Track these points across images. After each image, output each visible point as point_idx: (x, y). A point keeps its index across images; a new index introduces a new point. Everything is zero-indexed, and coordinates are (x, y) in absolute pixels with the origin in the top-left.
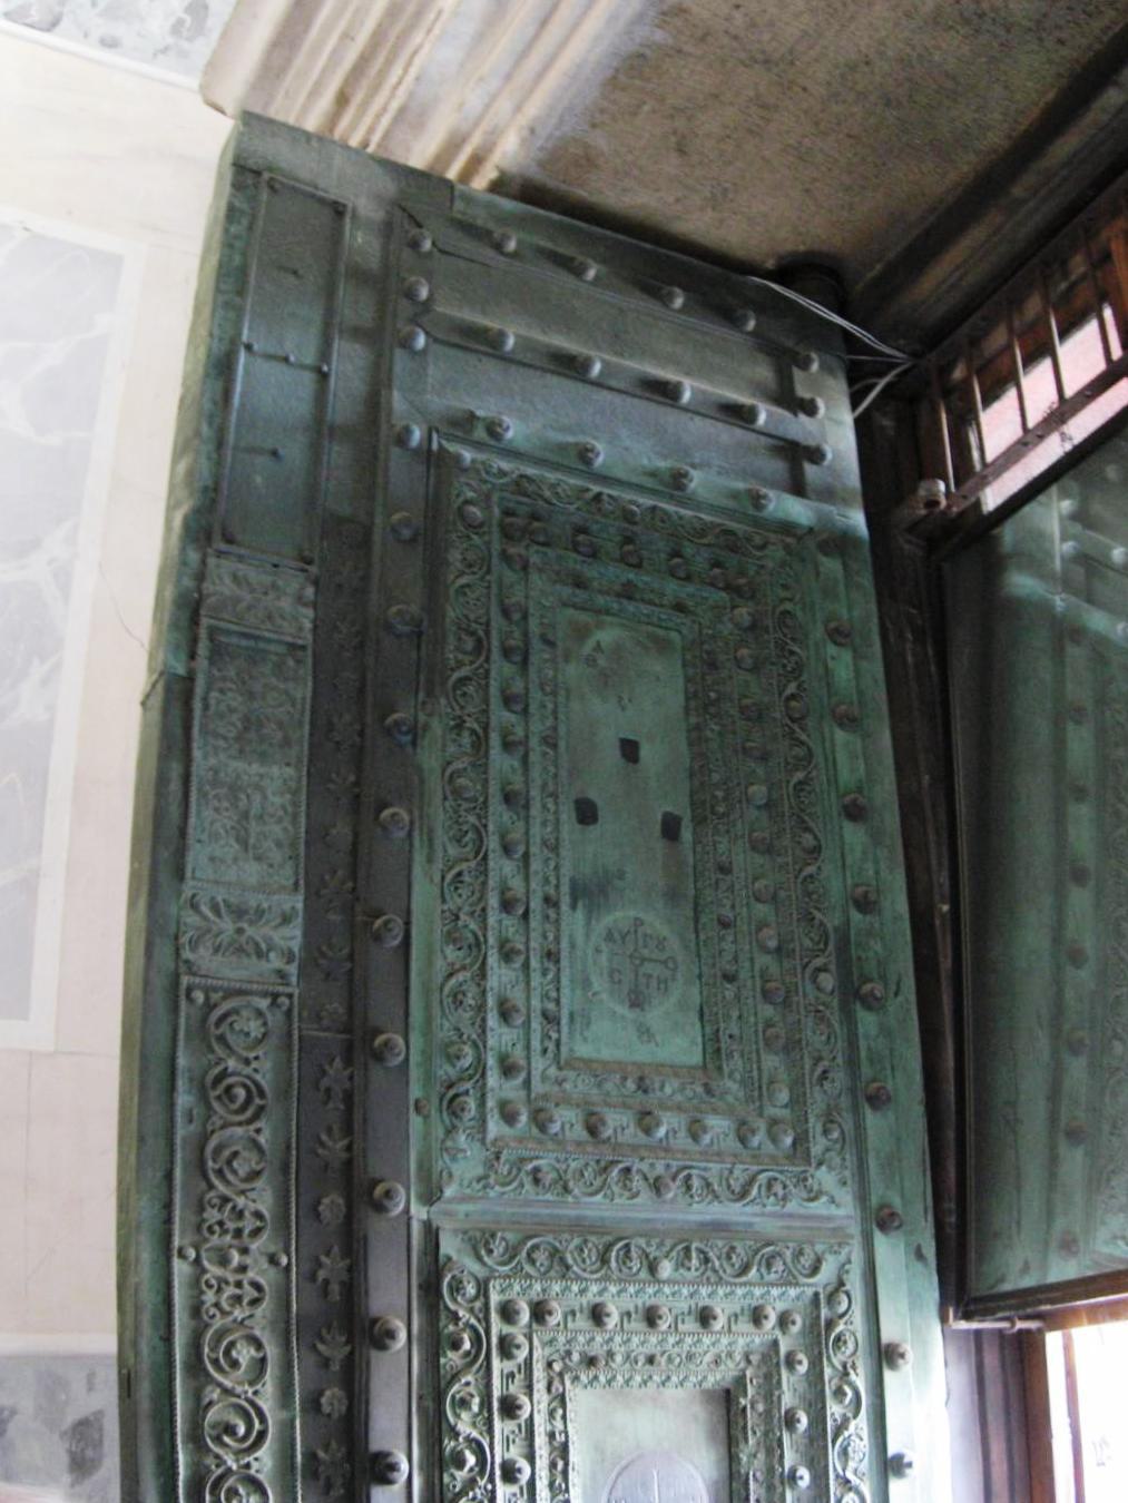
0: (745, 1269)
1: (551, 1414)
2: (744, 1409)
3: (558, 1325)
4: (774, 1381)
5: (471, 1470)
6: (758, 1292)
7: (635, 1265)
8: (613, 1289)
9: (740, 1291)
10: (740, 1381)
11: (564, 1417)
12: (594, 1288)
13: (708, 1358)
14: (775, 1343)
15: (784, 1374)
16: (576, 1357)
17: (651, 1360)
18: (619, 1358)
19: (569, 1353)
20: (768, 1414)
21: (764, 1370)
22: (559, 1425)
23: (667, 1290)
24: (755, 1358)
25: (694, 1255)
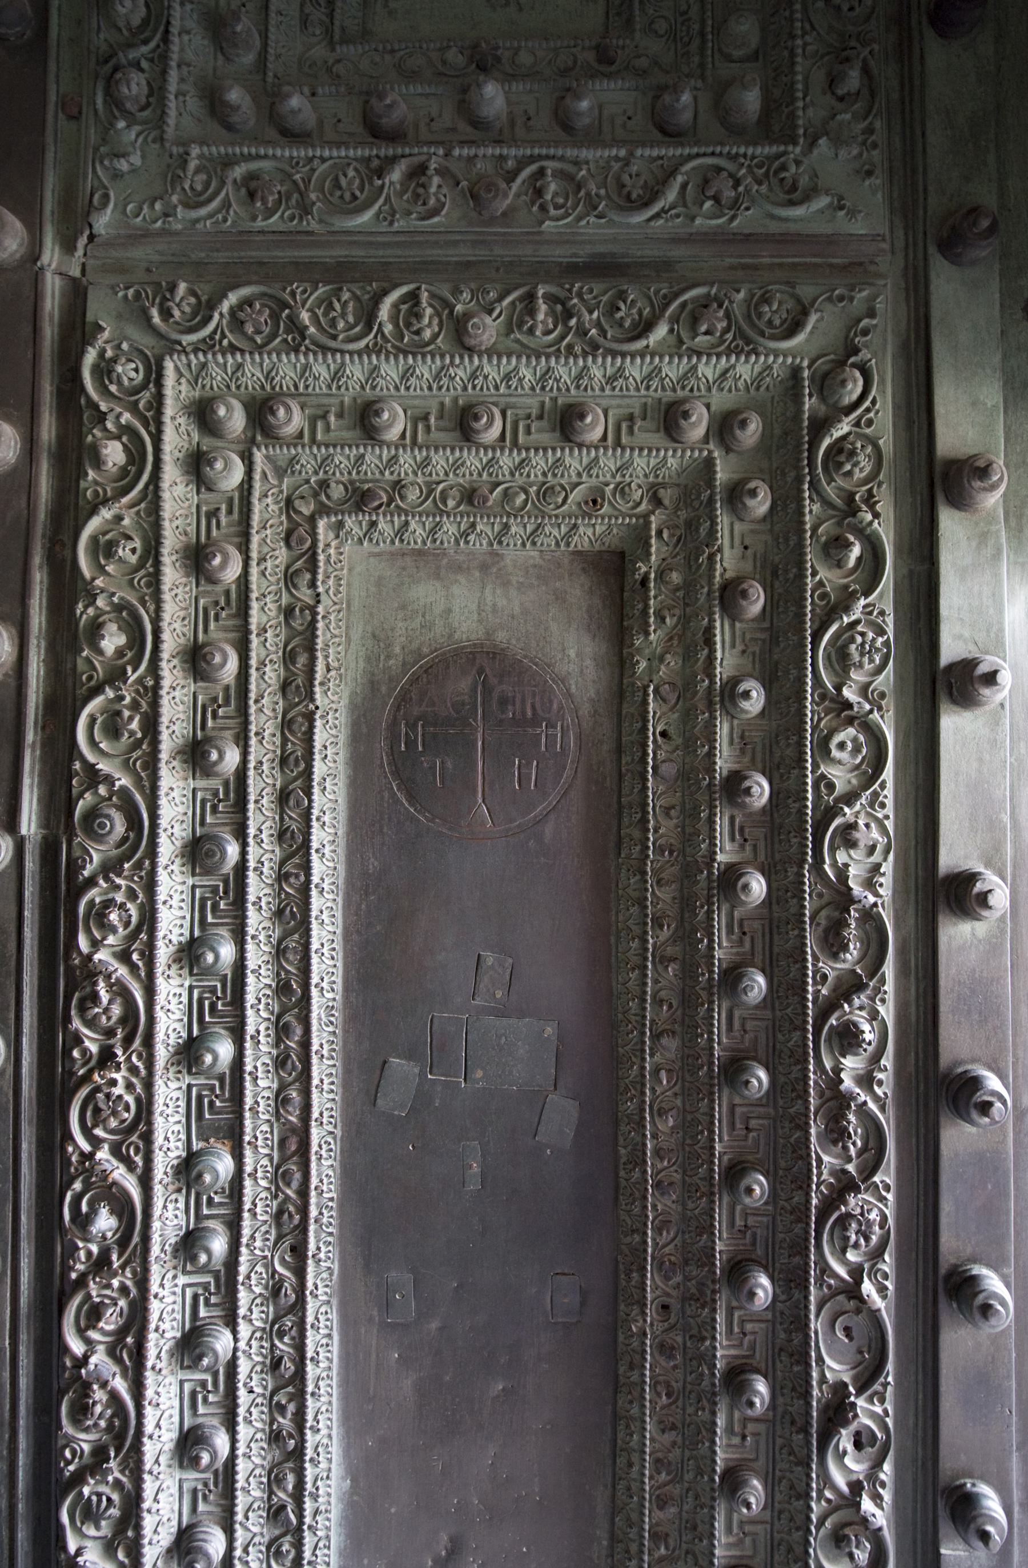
0: (645, 328)
1: (290, 578)
2: (644, 581)
3: (301, 435)
4: (703, 531)
5: (120, 653)
6: (672, 370)
7: (429, 324)
8: (390, 370)
9: (635, 370)
10: (640, 536)
11: (313, 584)
12: (356, 371)
13: (575, 496)
14: (709, 463)
15: (723, 520)
16: (337, 492)
17: (470, 496)
18: (413, 495)
19: (324, 484)
20: (689, 587)
21: (683, 514)
22: (305, 594)
23: (491, 371)
24: (667, 496)
25: (543, 307)
